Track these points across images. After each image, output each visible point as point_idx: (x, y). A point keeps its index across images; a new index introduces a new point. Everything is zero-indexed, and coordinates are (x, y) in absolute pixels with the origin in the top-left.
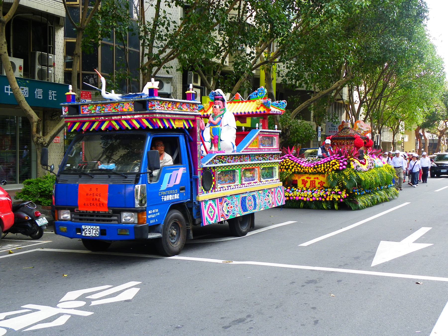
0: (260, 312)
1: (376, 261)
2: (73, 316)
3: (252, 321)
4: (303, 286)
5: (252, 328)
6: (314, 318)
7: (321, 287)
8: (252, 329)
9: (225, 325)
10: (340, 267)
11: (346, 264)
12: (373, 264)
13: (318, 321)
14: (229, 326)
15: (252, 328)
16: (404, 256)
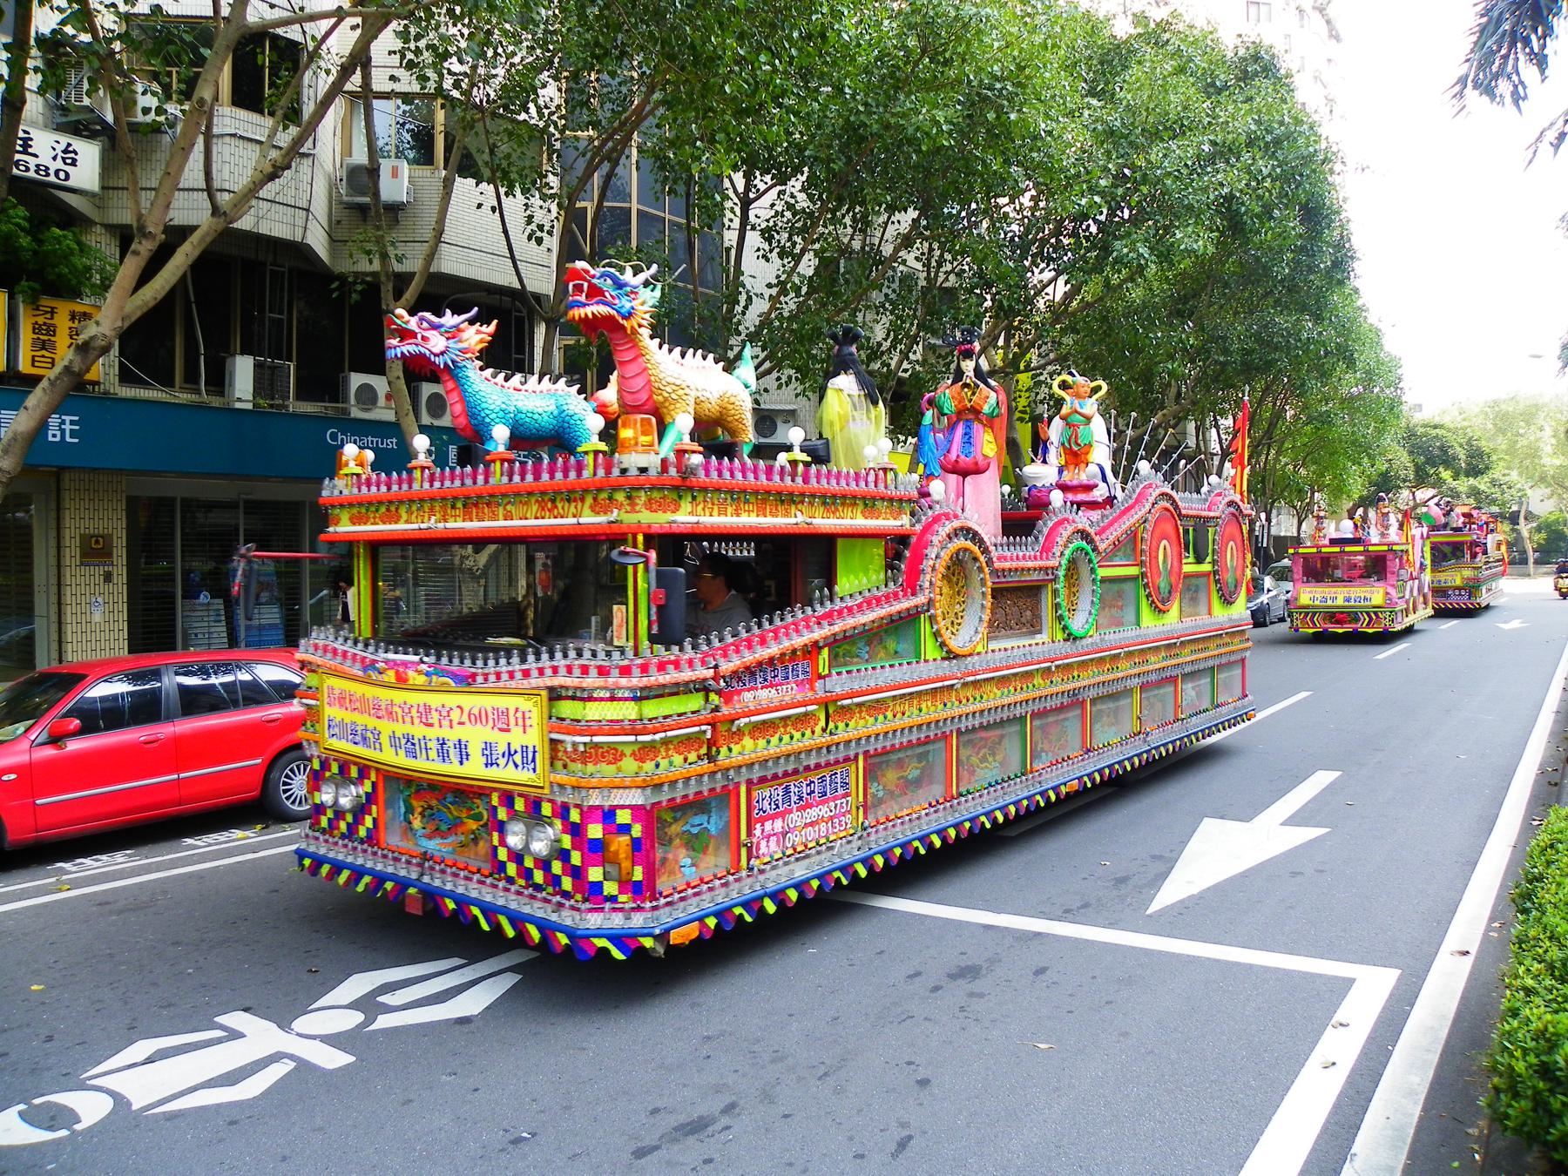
0: (768, 1097)
1: (1172, 892)
2: (303, 1066)
3: (728, 1128)
4: (936, 989)
5: (710, 1161)
6: (904, 1125)
7: (981, 995)
8: (706, 1167)
9: (647, 1142)
10: (1067, 915)
11: (1086, 906)
12: (1154, 907)
13: (910, 1138)
14: (657, 1148)
15: (710, 1161)
16: (1244, 875)
